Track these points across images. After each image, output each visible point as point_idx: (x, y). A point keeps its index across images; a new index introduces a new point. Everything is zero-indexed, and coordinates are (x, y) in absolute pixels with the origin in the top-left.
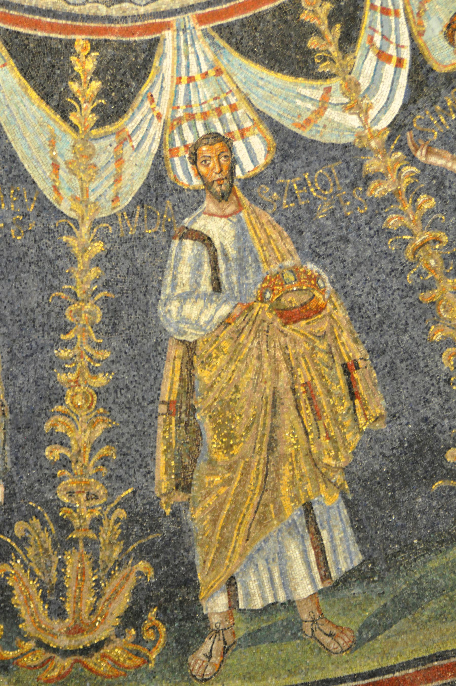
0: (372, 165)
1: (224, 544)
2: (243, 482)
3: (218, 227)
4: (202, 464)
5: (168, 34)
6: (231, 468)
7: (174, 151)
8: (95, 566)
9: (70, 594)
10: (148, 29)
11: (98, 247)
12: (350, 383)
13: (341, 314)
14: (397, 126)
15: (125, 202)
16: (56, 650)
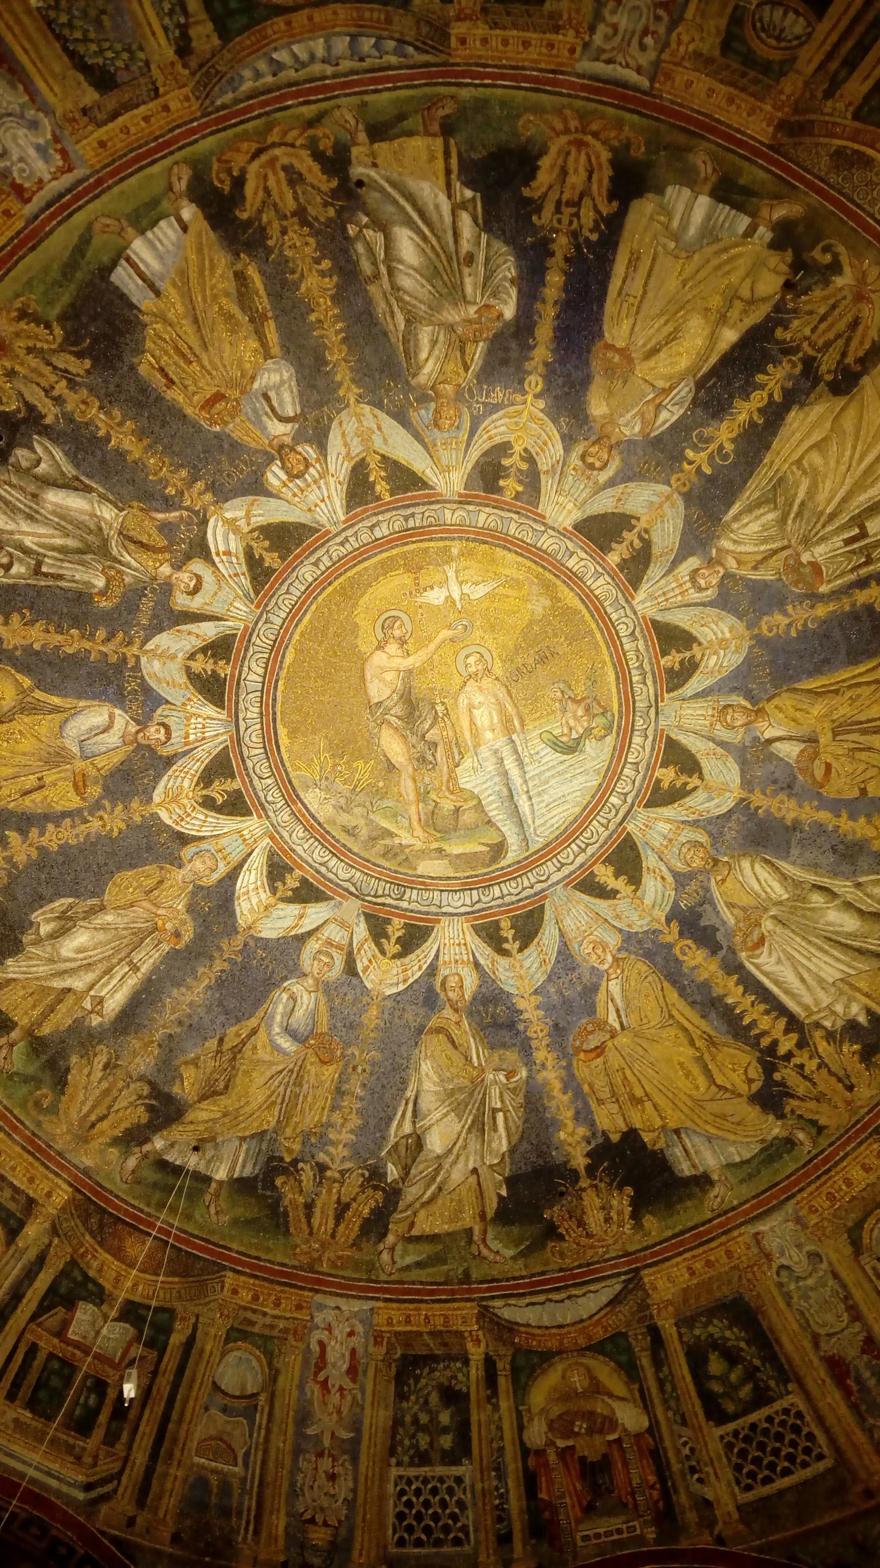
0: (208, 497)
1: (200, 250)
2: (204, 291)
3: (278, 429)
4: (233, 291)
5: (343, 518)
6: (215, 297)
7: (318, 460)
8: (275, 205)
9: (284, 184)
10: (355, 516)
11: (341, 393)
12: (166, 376)
13: (189, 411)
14: (204, 522)
15: (335, 424)
16: (280, 145)
